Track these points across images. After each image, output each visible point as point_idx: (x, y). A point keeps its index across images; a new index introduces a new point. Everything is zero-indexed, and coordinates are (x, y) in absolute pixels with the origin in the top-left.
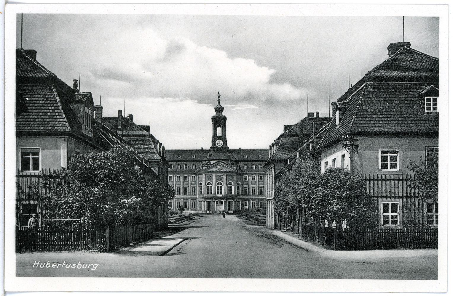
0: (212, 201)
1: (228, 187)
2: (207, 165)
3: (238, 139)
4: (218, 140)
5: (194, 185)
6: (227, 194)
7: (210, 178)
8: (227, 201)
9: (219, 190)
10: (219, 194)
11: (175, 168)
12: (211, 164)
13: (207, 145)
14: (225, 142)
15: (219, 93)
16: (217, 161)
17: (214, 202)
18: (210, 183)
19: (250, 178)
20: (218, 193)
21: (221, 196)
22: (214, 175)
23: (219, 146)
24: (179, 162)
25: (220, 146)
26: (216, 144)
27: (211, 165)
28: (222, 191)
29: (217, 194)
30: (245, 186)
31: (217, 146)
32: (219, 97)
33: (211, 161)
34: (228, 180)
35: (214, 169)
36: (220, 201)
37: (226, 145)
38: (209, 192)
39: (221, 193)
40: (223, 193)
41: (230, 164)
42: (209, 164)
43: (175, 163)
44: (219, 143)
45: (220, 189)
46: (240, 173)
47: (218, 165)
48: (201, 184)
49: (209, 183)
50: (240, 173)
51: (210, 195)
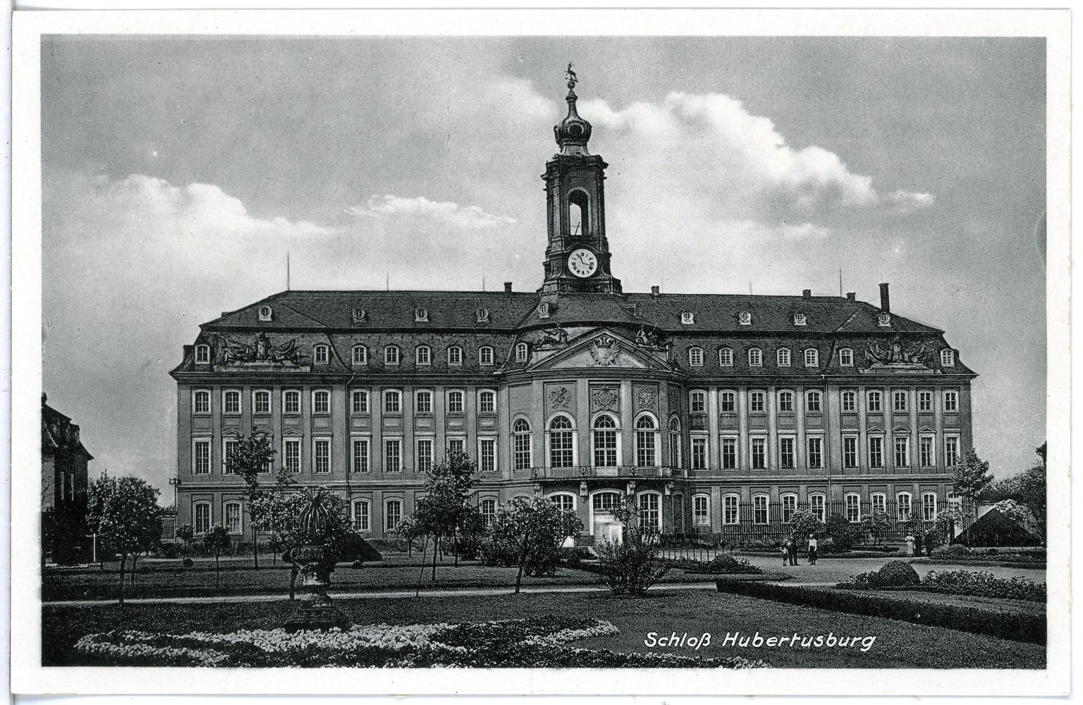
0: (574, 496)
1: (640, 434)
3: (667, 243)
4: (579, 252)
5: (489, 428)
6: (636, 464)
7: (561, 396)
8: (639, 495)
9: (605, 450)
10: (603, 464)
11: (407, 360)
12: (570, 338)
13: (529, 277)
14: (604, 259)
15: (572, 69)
16: (586, 329)
17: (587, 498)
18: (565, 419)
19: (712, 399)
20: (599, 462)
21: (610, 472)
22: (583, 384)
23: (580, 275)
24: (425, 337)
25: (586, 275)
26: (571, 267)
27: (569, 343)
28: (614, 452)
29: (597, 464)
30: (696, 435)
31: (575, 272)
32: (571, 86)
33: (569, 330)
34: (637, 406)
35: (583, 360)
36: (610, 494)
37: (608, 271)
38: (561, 456)
39: (612, 463)
40: (619, 461)
41: (645, 340)
42: (557, 338)
43: (407, 338)
44: (583, 264)
45: (608, 446)
46: (684, 384)
47: (597, 343)
48: (521, 424)
49: (560, 422)
50: (684, 384)
51: (562, 473)
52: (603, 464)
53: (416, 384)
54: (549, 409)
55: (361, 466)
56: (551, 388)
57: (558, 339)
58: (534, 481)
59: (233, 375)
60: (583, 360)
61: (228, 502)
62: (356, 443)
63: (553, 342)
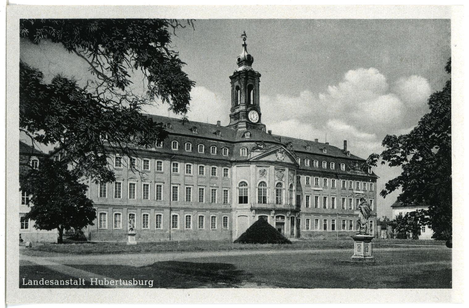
2: (258, 150)
7: (263, 173)
17: (273, 217)
22: (272, 167)
35: (272, 158)
38: (262, 199)
42: (262, 147)
52: (278, 203)
53: (211, 164)
54: (258, 178)
55: (175, 197)
56: (259, 169)
57: (262, 148)
58: (252, 209)
59: (154, 152)
60: (272, 158)
61: (130, 213)
62: (173, 187)
63: (260, 149)
